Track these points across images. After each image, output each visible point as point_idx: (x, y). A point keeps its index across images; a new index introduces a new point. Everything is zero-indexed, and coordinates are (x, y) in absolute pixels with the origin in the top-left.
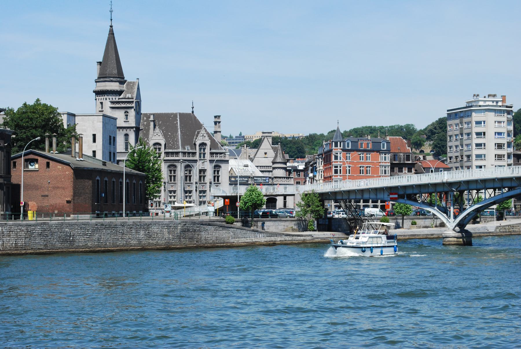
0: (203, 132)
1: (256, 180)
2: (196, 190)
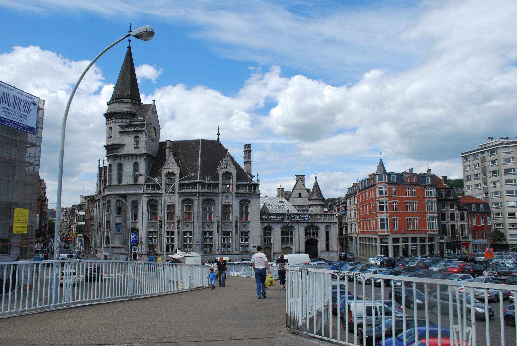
0: (226, 159)
1: (293, 218)
2: (218, 231)
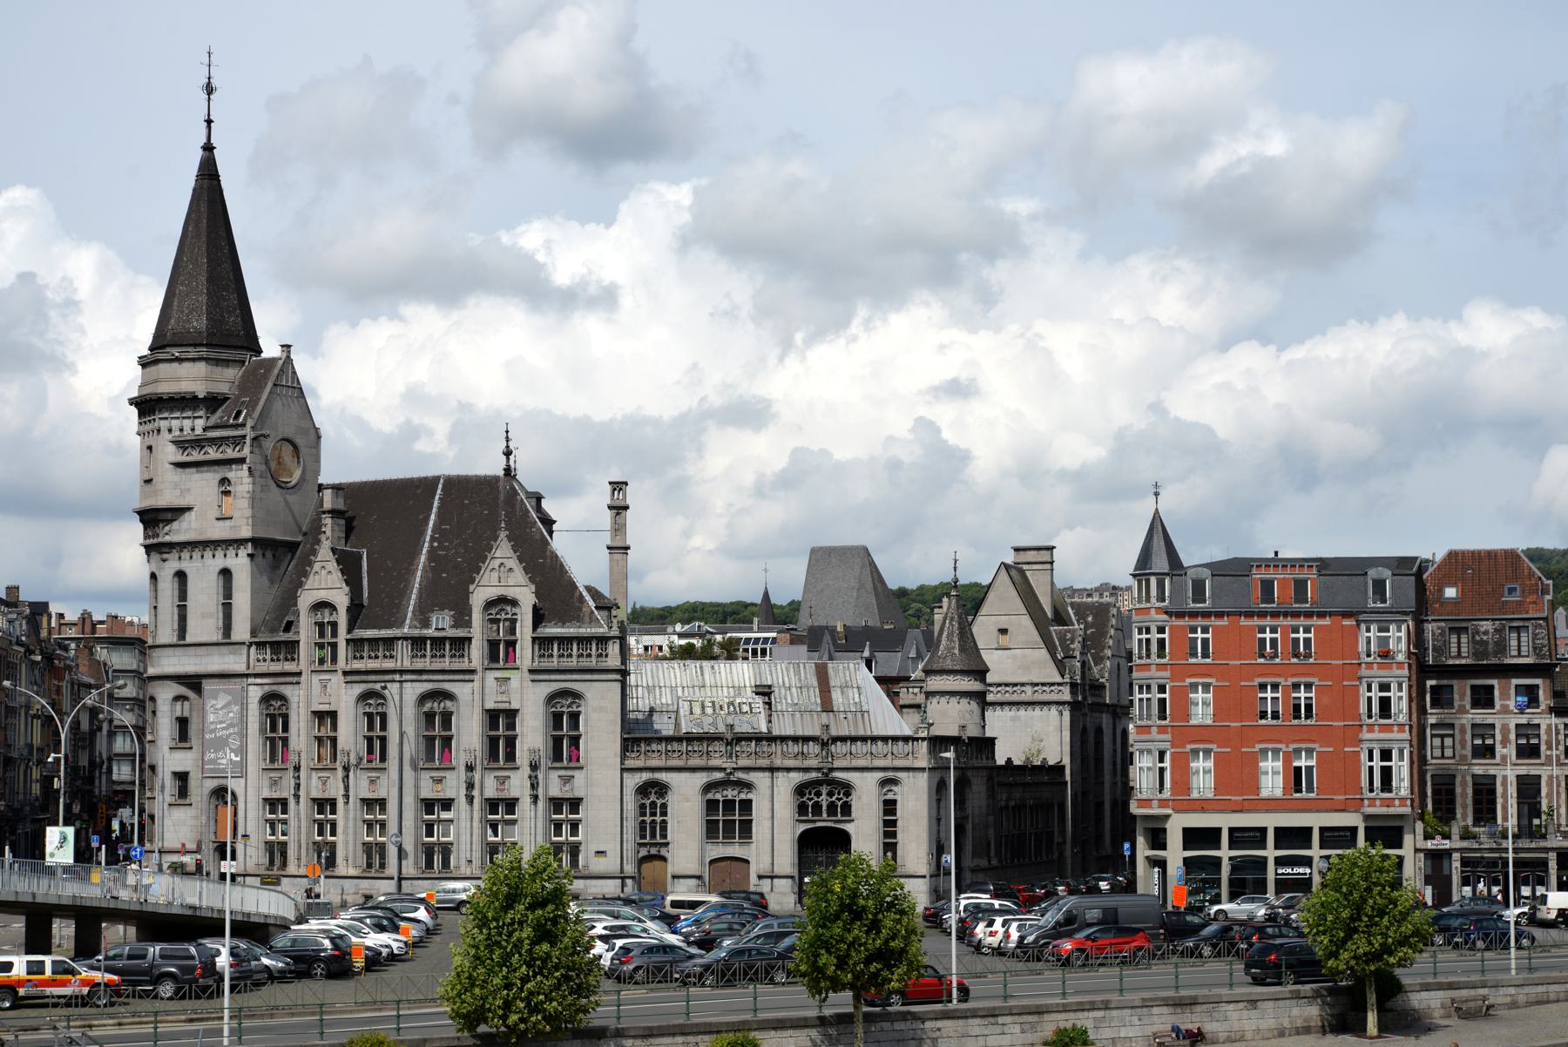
0: (503, 551)
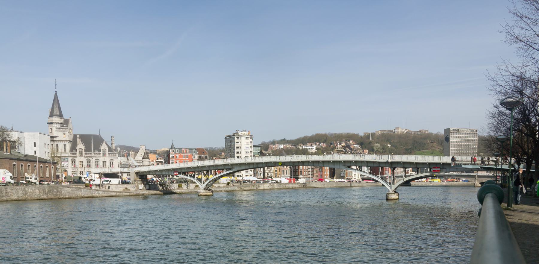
0: (104, 144)
